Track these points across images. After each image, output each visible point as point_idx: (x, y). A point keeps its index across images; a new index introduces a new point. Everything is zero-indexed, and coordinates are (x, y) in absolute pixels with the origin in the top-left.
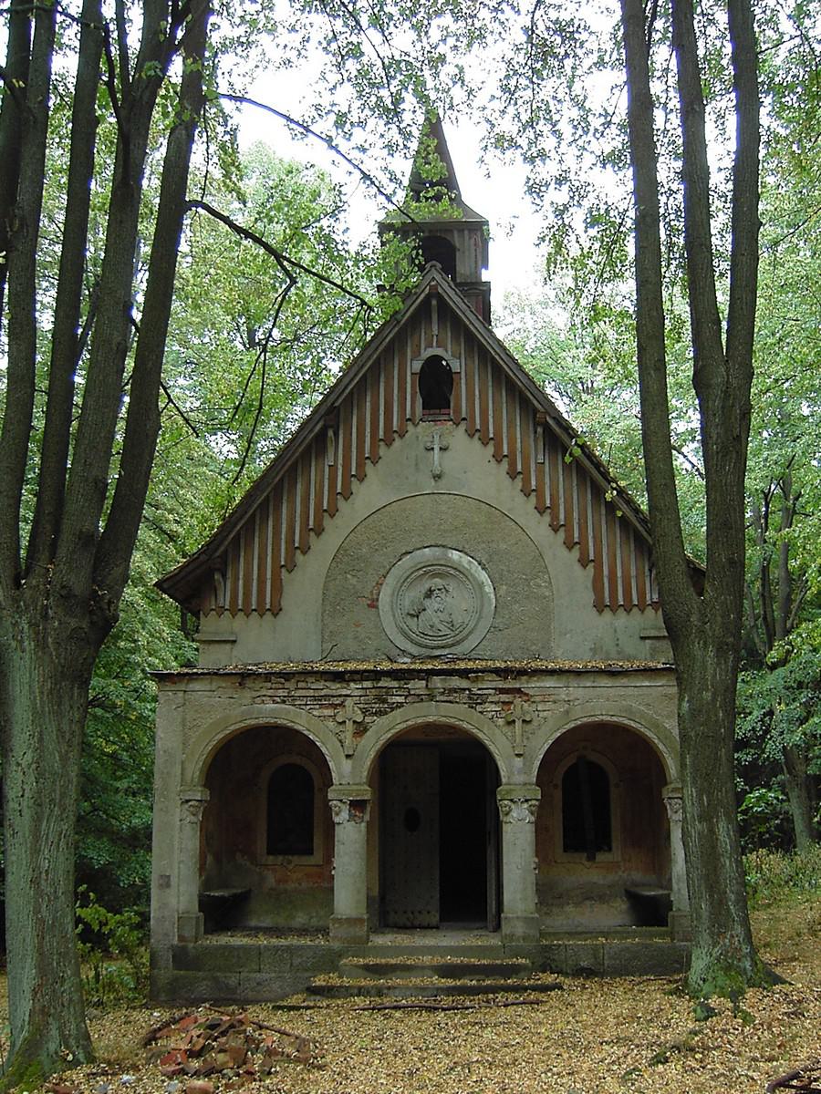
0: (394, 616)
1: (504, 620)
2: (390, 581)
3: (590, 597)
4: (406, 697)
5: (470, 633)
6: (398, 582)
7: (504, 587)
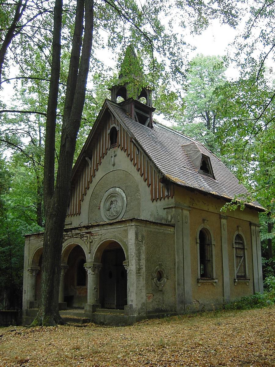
2: (103, 200)
3: (150, 197)
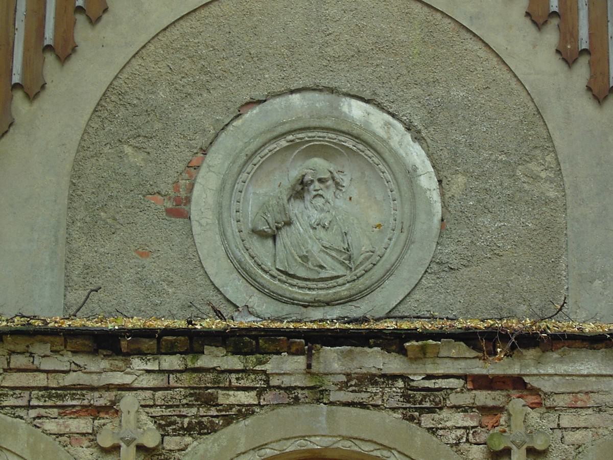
0: (223, 234)
1: (460, 248)
2: (217, 159)
4: (260, 392)
5: (389, 273)
6: (234, 162)
7: (461, 179)
